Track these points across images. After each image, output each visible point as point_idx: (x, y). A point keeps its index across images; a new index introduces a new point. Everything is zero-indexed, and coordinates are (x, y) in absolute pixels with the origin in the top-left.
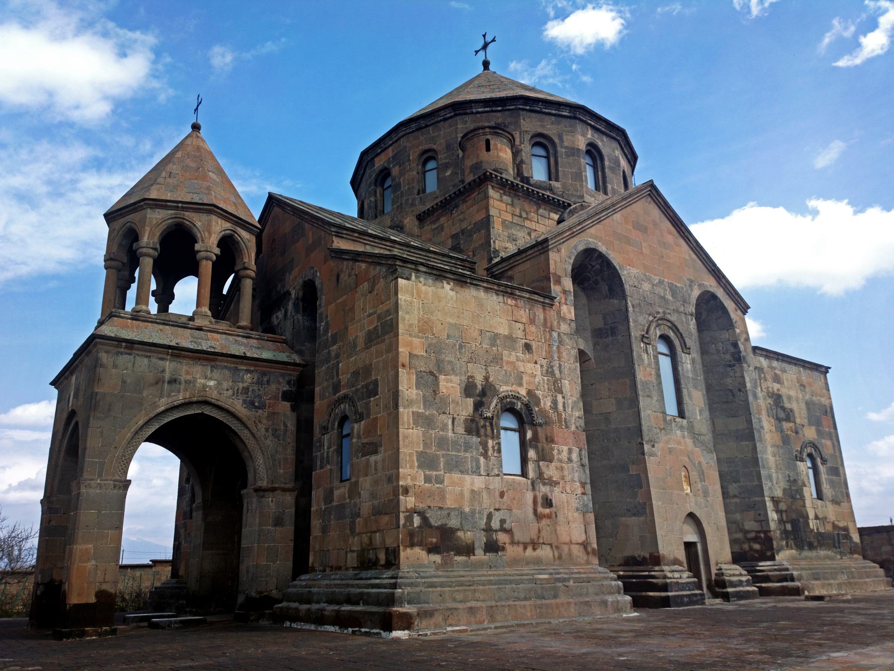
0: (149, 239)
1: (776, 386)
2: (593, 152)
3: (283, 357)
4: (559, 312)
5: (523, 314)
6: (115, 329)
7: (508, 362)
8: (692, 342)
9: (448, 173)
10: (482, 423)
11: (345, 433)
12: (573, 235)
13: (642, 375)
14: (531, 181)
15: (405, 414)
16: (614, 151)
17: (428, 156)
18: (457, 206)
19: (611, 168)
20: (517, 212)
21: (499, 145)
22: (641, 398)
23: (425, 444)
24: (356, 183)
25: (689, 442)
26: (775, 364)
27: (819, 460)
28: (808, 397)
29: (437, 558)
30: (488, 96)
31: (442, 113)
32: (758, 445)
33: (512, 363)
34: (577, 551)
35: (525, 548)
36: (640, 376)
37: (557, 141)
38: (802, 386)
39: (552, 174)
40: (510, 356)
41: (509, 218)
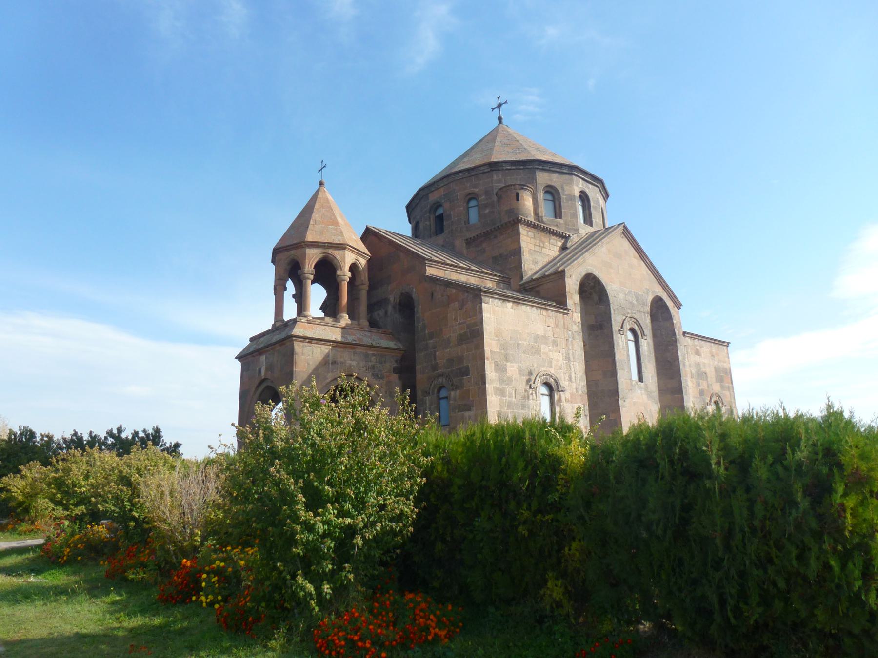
0: (309, 267)
1: (697, 358)
2: (584, 198)
3: (392, 344)
5: (551, 321)
6: (302, 330)
7: (544, 353)
8: (648, 331)
9: (487, 211)
10: (531, 391)
11: (441, 396)
13: (619, 356)
14: (545, 219)
15: (490, 387)
17: (471, 197)
18: (496, 237)
21: (525, 197)
22: (618, 371)
23: (502, 407)
24: (410, 208)
25: (645, 397)
26: (697, 342)
27: (721, 405)
28: (716, 363)
30: (513, 159)
31: (482, 168)
33: (546, 353)
36: (618, 357)
37: (560, 190)
39: (558, 214)
40: (545, 349)
41: (532, 247)
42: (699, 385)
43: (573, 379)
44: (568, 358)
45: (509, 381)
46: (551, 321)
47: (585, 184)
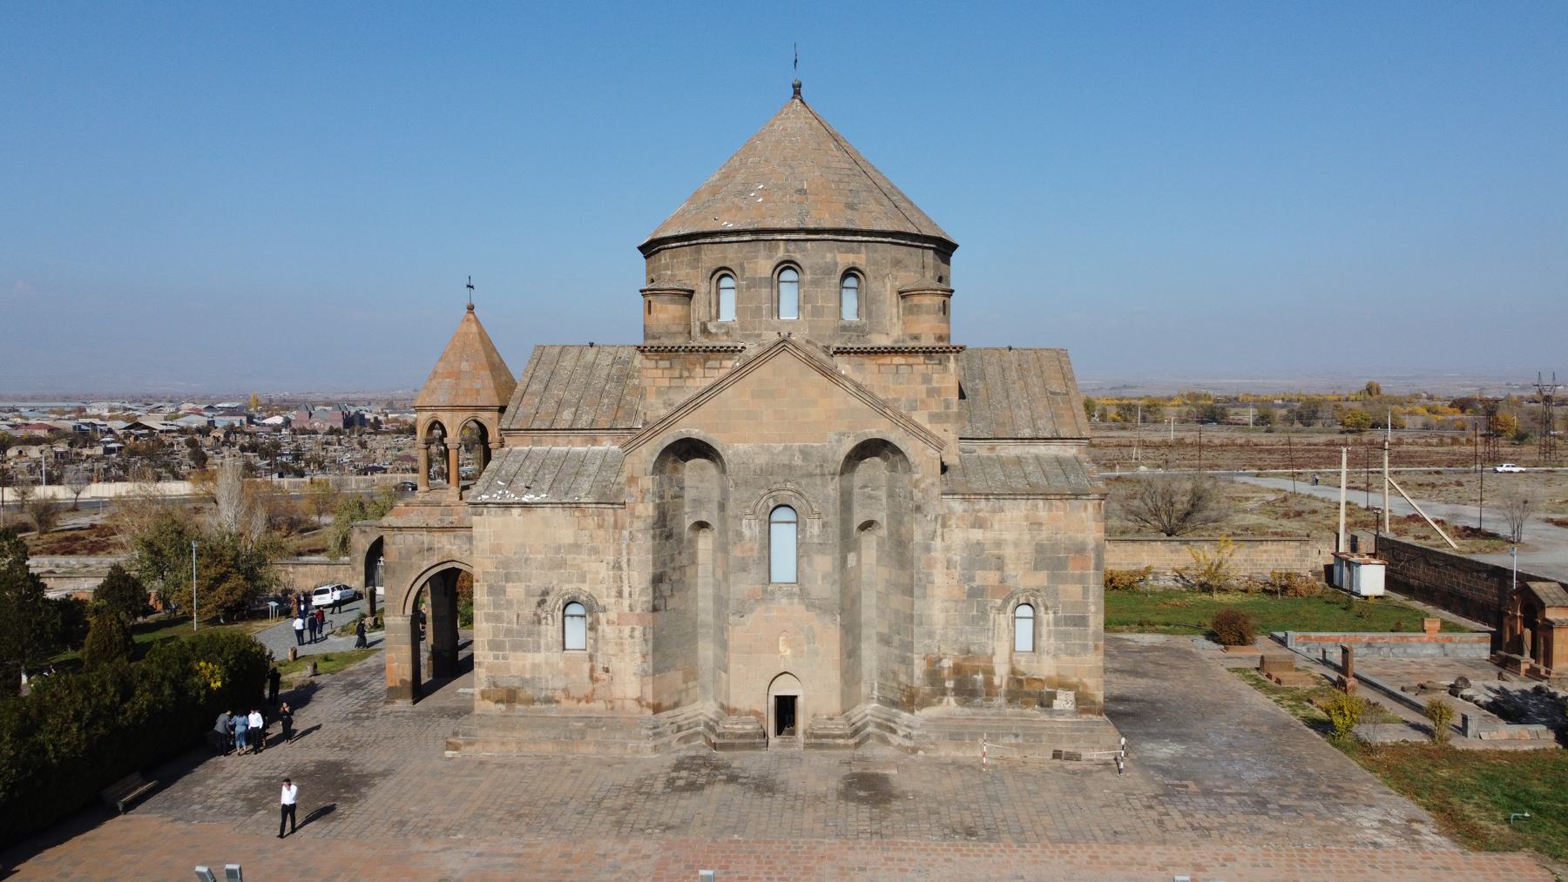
1: (976, 535)
4: (632, 515)
5: (591, 522)
12: (656, 434)
16: (824, 257)
19: (815, 283)
20: (677, 373)
25: (798, 608)
28: (1044, 535)
29: (502, 707)
32: (918, 604)
34: (632, 706)
35: (579, 701)
38: (1036, 524)
41: (666, 383)
42: (971, 579)
43: (626, 594)
44: (617, 566)
45: (510, 603)
46: (591, 522)
47: (792, 246)
